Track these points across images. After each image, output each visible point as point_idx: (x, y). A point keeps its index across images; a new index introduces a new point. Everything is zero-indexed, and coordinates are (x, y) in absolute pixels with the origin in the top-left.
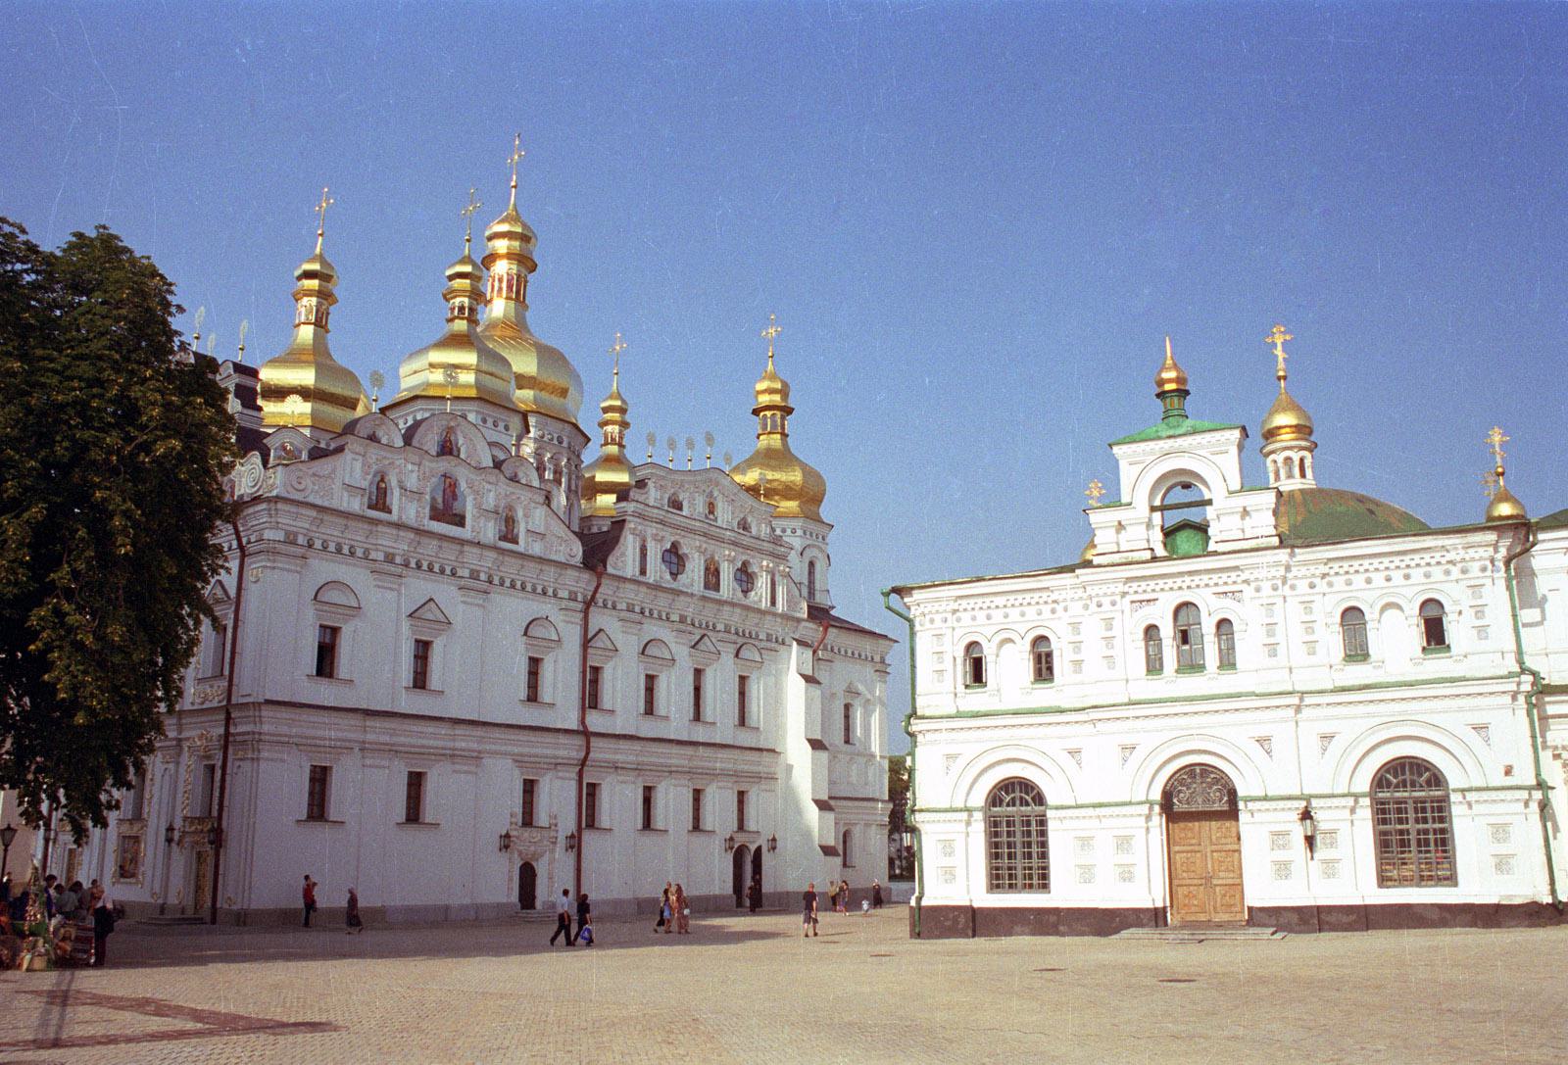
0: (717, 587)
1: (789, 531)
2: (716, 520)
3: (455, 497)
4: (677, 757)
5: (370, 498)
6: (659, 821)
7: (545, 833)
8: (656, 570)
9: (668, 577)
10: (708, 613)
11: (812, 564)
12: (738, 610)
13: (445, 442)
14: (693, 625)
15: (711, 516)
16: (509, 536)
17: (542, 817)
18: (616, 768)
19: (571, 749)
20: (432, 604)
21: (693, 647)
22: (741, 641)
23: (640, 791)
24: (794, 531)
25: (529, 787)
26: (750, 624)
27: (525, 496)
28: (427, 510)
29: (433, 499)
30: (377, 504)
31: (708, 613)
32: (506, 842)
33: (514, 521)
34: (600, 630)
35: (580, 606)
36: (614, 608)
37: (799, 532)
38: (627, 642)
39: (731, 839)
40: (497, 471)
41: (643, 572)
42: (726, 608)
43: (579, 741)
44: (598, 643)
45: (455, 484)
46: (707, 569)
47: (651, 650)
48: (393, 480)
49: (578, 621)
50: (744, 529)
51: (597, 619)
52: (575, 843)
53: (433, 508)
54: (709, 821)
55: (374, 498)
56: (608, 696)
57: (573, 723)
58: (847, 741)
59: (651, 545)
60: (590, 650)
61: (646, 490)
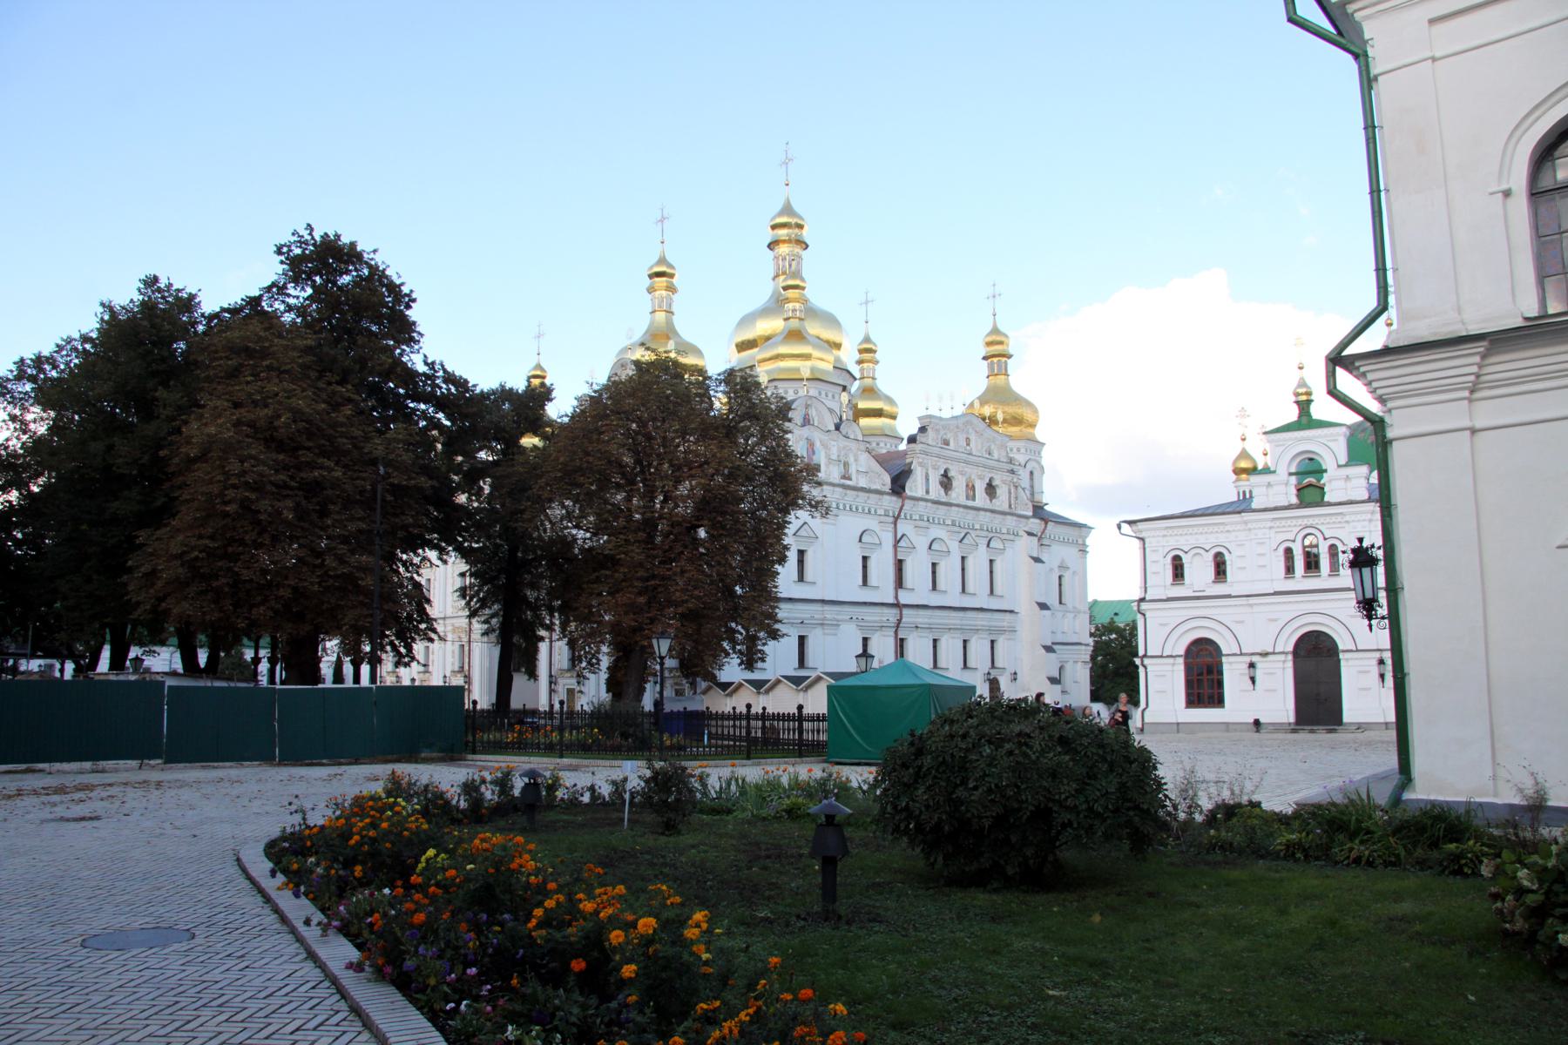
0: (974, 498)
1: (1015, 450)
3: (814, 453)
8: (936, 492)
11: (1031, 473)
12: (988, 514)
16: (846, 477)
19: (891, 615)
20: (806, 526)
22: (991, 535)
24: (1018, 450)
27: (853, 445)
35: (891, 519)
37: (1023, 450)
39: (989, 673)
41: (927, 492)
43: (895, 611)
46: (967, 486)
50: (989, 454)
51: (903, 527)
57: (891, 600)
58: (1061, 603)
60: (899, 549)
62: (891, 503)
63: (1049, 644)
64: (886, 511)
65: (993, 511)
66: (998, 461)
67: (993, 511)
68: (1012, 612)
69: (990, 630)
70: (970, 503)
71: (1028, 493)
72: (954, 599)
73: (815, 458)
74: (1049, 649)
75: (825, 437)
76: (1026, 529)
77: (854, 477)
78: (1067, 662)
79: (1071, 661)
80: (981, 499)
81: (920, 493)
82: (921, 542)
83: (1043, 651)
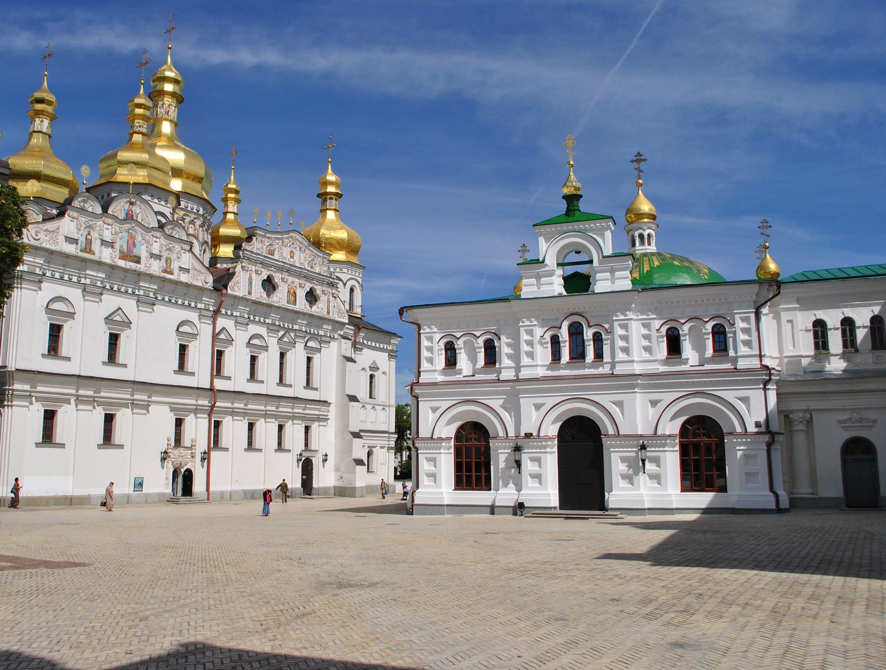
0: (295, 303)
3: (134, 245)
5: (81, 244)
6: (257, 444)
8: (259, 293)
9: (264, 295)
13: (129, 211)
15: (292, 260)
17: (186, 441)
18: (233, 413)
20: (120, 311)
25: (179, 423)
28: (117, 253)
29: (121, 246)
30: (85, 249)
33: (171, 261)
34: (224, 329)
38: (241, 336)
39: (301, 455)
41: (250, 293)
44: (222, 336)
45: (135, 237)
46: (289, 292)
48: (95, 235)
49: (211, 322)
51: (221, 322)
52: (206, 457)
53: (121, 252)
54: (287, 445)
55: (84, 245)
57: (208, 386)
58: (371, 397)
61: (251, 243)
69: (303, 418)
70: (291, 307)
71: (347, 307)
73: (135, 250)
74: (356, 435)
78: (375, 447)
79: (379, 446)
80: (302, 304)
83: (351, 436)
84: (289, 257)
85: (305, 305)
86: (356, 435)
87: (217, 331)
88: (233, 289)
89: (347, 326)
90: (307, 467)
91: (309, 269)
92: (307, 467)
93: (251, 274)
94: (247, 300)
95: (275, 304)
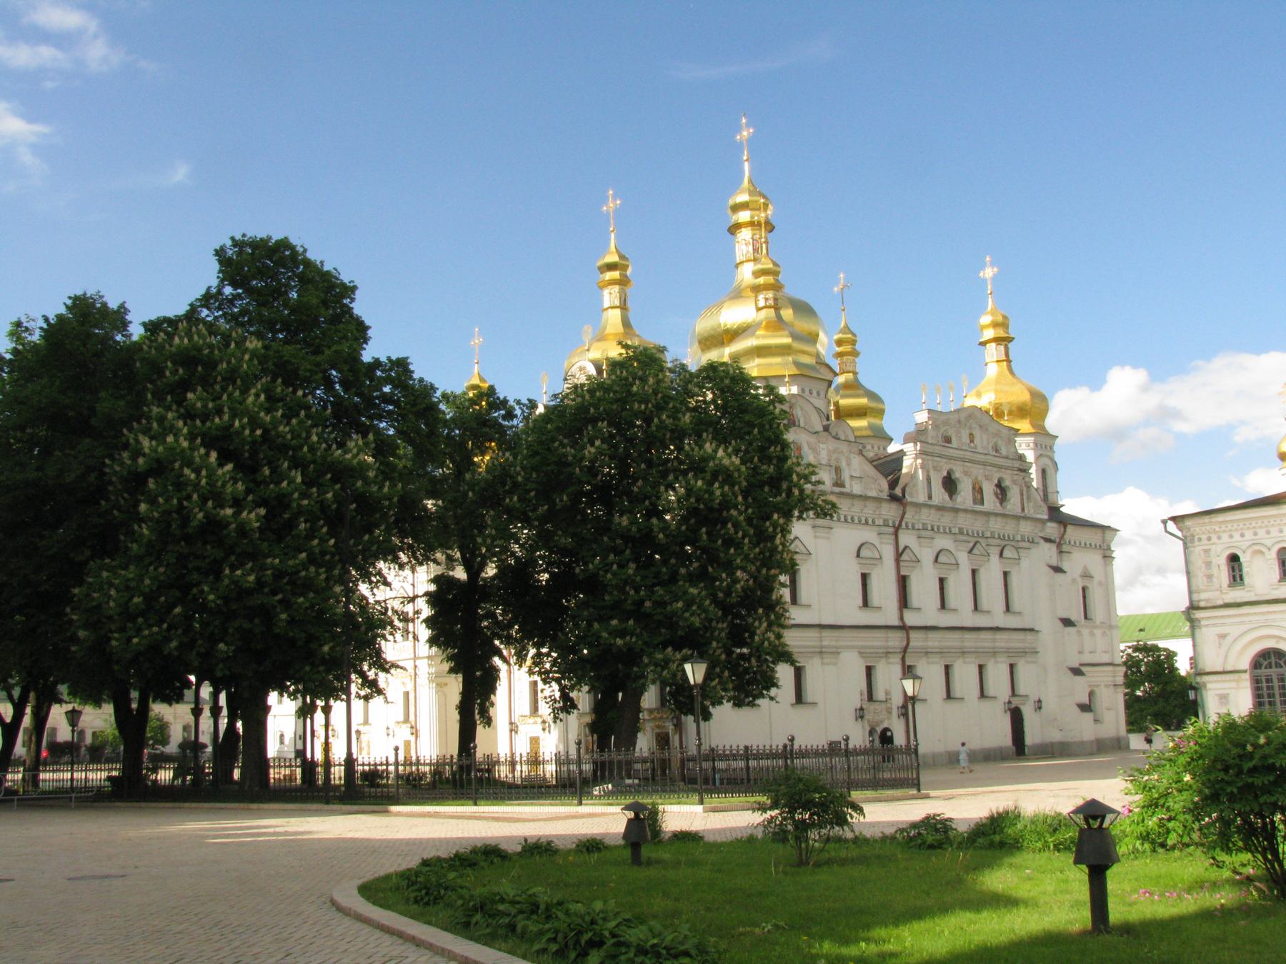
0: (982, 503)
2: (976, 447)
4: (970, 640)
6: (957, 690)
7: (883, 706)
8: (940, 495)
9: (946, 497)
10: (978, 525)
12: (999, 519)
14: (968, 534)
17: (880, 694)
19: (896, 640)
21: (970, 552)
22: (1003, 543)
23: (943, 669)
26: (1008, 528)
27: (844, 447)
31: (978, 525)
32: (860, 714)
34: (906, 547)
35: (891, 530)
36: (913, 528)
39: (1010, 702)
40: (826, 433)
41: (930, 497)
42: (992, 519)
44: (904, 557)
46: (974, 488)
47: (942, 558)
51: (906, 538)
54: (991, 689)
56: (915, 597)
57: (895, 621)
58: (1086, 617)
59: (932, 473)
60: (902, 564)
62: (890, 512)
63: (1076, 665)
64: (885, 520)
65: (1004, 516)
66: (1007, 458)
67: (1004, 516)
68: (1032, 630)
69: (1008, 652)
70: (978, 508)
71: (1042, 494)
72: (966, 617)
74: (1077, 672)
75: (812, 439)
76: (1042, 535)
77: (847, 485)
78: (1098, 686)
80: (990, 502)
81: (922, 498)
82: (927, 555)
84: (968, 441)
85: (994, 502)
86: (1077, 672)
87: (901, 549)
88: (912, 496)
89: (1049, 524)
90: (1017, 718)
91: (994, 453)
92: (1017, 718)
93: (928, 472)
94: (930, 506)
95: (960, 507)
